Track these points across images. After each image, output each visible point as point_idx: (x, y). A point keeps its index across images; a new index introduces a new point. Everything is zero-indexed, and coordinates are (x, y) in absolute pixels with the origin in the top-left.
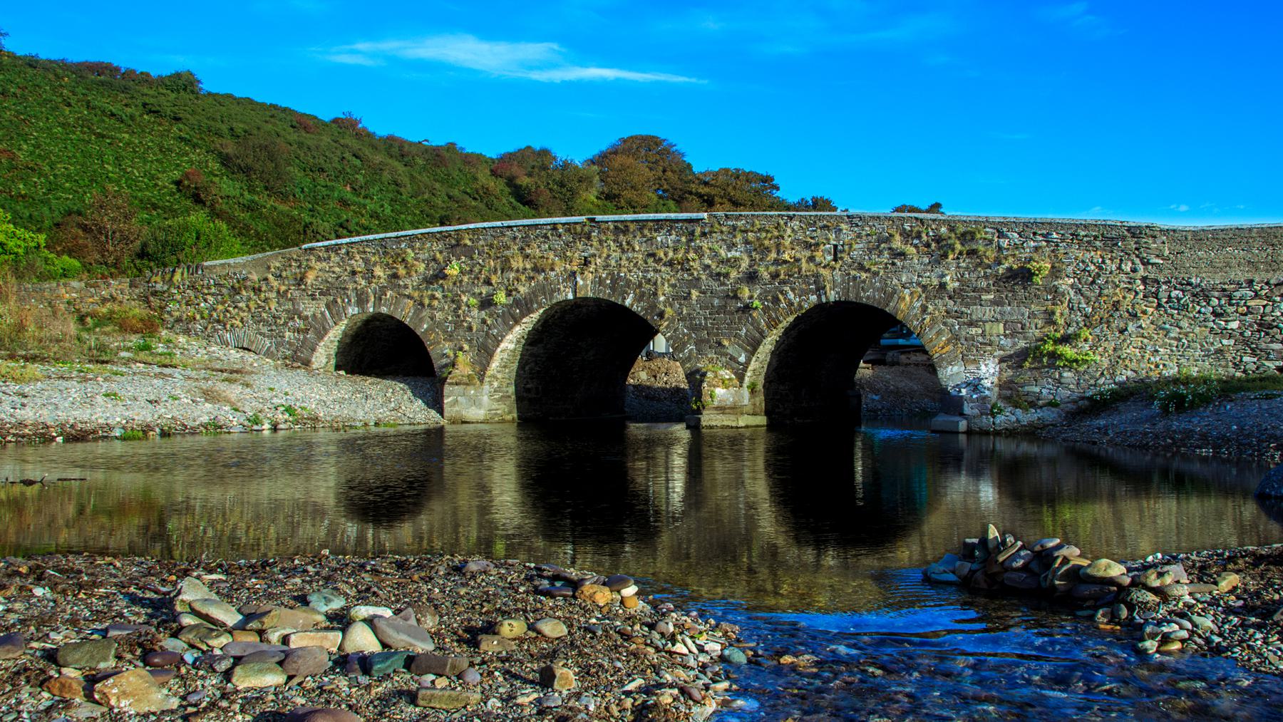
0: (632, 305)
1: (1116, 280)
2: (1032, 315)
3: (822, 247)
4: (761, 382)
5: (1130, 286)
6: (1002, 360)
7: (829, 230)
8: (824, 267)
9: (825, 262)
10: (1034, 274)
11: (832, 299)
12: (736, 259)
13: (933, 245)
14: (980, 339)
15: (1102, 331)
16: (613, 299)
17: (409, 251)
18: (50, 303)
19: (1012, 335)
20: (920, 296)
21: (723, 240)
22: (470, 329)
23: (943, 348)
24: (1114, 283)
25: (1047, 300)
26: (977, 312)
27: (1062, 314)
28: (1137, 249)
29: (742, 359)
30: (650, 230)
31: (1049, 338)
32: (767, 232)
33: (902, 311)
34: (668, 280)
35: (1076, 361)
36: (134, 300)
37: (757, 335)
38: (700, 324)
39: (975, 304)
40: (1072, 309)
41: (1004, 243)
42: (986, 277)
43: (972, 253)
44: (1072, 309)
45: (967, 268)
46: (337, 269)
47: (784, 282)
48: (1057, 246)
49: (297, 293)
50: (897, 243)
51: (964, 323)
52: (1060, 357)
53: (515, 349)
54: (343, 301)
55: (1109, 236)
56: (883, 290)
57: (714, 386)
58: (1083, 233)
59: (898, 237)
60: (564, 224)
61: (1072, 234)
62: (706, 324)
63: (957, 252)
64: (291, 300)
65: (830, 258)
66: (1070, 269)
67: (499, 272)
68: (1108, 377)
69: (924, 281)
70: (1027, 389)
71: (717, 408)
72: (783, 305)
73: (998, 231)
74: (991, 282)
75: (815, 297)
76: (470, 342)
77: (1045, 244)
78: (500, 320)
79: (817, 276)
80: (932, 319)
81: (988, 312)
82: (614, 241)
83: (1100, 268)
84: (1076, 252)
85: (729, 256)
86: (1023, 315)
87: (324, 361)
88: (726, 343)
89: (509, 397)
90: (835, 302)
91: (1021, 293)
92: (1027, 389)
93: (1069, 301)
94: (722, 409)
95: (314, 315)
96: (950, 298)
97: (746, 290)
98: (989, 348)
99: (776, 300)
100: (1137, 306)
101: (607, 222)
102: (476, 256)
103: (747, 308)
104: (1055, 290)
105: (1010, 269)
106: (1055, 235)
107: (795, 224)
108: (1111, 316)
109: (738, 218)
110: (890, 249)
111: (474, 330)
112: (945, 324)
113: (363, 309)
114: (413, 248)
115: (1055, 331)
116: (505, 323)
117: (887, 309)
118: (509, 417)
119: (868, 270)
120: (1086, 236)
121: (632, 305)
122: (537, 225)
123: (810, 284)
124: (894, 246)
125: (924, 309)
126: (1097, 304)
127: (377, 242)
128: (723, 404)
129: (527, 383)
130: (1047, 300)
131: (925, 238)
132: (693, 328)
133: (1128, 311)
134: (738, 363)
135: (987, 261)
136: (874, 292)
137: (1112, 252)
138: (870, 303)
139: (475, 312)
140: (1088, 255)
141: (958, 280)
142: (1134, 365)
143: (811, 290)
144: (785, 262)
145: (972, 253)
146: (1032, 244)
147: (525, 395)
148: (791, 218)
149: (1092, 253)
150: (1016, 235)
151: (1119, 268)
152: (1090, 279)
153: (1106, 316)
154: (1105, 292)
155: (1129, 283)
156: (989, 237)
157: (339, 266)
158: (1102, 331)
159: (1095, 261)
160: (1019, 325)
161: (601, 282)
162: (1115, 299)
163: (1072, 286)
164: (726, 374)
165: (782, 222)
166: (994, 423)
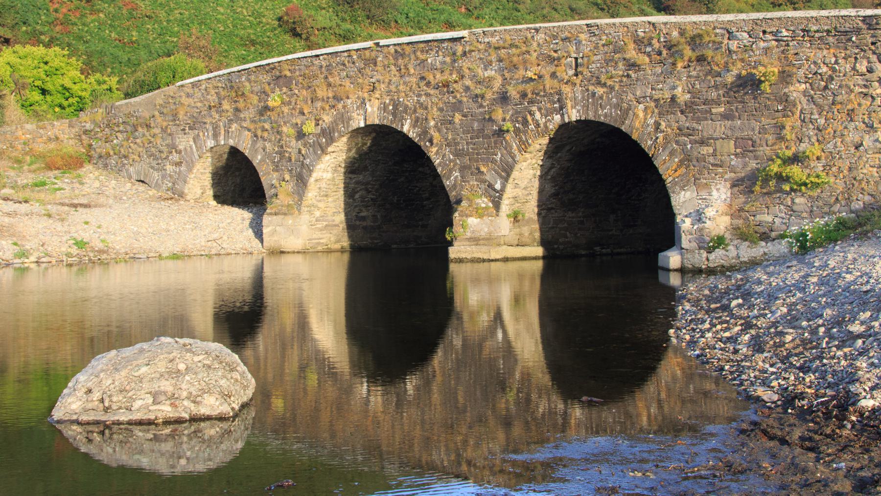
0: (409, 131)
1: (851, 84)
2: (763, 130)
3: (563, 61)
4: (531, 209)
5: (864, 90)
6: (733, 186)
7: (570, 42)
8: (566, 83)
9: (566, 78)
10: (761, 82)
11: (574, 119)
12: (490, 79)
13: (665, 52)
14: (711, 160)
15: (835, 147)
16: (394, 126)
17: (247, 84)
18: (11, 144)
19: (743, 155)
20: (653, 112)
21: (481, 59)
22: (290, 159)
23: (676, 171)
24: (847, 86)
25: (778, 111)
26: (707, 128)
27: (793, 128)
28: (873, 44)
29: (498, 186)
30: (422, 51)
31: (778, 157)
32: (517, 47)
33: (637, 130)
34: (437, 104)
35: (805, 184)
36: (72, 139)
37: (510, 160)
38: (463, 150)
39: (706, 119)
40: (803, 121)
41: (734, 45)
42: (716, 87)
43: (701, 59)
44: (803, 121)
45: (698, 77)
46: (199, 105)
47: (531, 102)
48: (788, 45)
49: (174, 128)
50: (632, 53)
51: (696, 142)
52: (787, 179)
53: (334, 178)
54: (204, 135)
55: (842, 29)
56: (618, 106)
57: (467, 216)
58: (814, 28)
59: (632, 46)
60: (357, 50)
61: (803, 30)
62: (468, 149)
63: (686, 58)
64: (170, 135)
65: (571, 72)
66: (801, 73)
67: (310, 102)
68: (843, 203)
69: (657, 95)
70: (759, 218)
71: (469, 239)
72: (532, 127)
73: (729, 32)
74: (721, 92)
75: (559, 116)
76: (290, 171)
77: (774, 43)
78: (311, 149)
79: (559, 93)
80: (665, 138)
81: (719, 128)
82: (395, 65)
83: (834, 70)
84: (807, 51)
85: (486, 75)
86: (753, 130)
87: (199, 192)
88: (483, 169)
89: (337, 225)
90: (577, 121)
91: (751, 104)
92: (759, 218)
93: (801, 112)
94: (475, 241)
95: (185, 149)
96: (682, 112)
97: (500, 111)
98: (720, 170)
99: (525, 123)
100: (873, 114)
101: (388, 46)
102: (293, 86)
103: (501, 132)
104: (785, 99)
105: (739, 76)
106: (785, 33)
107: (540, 37)
108: (846, 128)
109: (493, 34)
110: (625, 59)
111: (293, 160)
112: (677, 143)
113: (217, 141)
114: (249, 81)
115: (787, 148)
116: (315, 153)
117: (623, 128)
118: (338, 246)
119: (604, 85)
120: (817, 31)
121: (409, 131)
122: (337, 53)
123: (555, 103)
124: (627, 56)
125: (657, 125)
126: (830, 114)
127: (225, 77)
128: (477, 235)
129: (361, 211)
130: (778, 111)
131: (656, 45)
132: (458, 154)
133: (864, 123)
134: (495, 190)
135: (716, 68)
136: (611, 109)
137: (846, 49)
138: (607, 121)
139: (293, 143)
140: (820, 54)
141: (689, 92)
142: (871, 188)
143: (555, 109)
144: (531, 80)
145: (701, 59)
146: (762, 44)
147: (358, 223)
148: (537, 30)
149: (825, 52)
150: (745, 35)
151: (854, 68)
152: (823, 84)
153: (840, 128)
154: (839, 98)
155: (865, 86)
156: (719, 39)
157: (201, 101)
158: (835, 147)
159: (827, 61)
160: (750, 142)
161: (385, 109)
162: (849, 107)
163: (805, 93)
164: (484, 202)
165: (529, 36)
166: (708, 259)
